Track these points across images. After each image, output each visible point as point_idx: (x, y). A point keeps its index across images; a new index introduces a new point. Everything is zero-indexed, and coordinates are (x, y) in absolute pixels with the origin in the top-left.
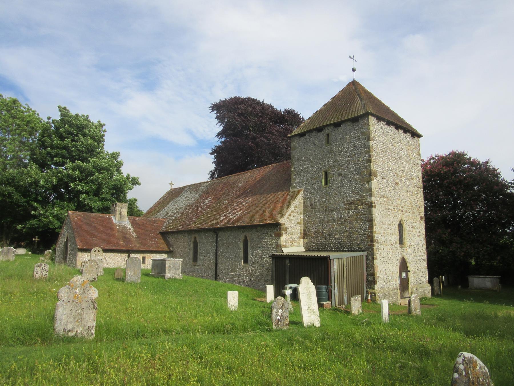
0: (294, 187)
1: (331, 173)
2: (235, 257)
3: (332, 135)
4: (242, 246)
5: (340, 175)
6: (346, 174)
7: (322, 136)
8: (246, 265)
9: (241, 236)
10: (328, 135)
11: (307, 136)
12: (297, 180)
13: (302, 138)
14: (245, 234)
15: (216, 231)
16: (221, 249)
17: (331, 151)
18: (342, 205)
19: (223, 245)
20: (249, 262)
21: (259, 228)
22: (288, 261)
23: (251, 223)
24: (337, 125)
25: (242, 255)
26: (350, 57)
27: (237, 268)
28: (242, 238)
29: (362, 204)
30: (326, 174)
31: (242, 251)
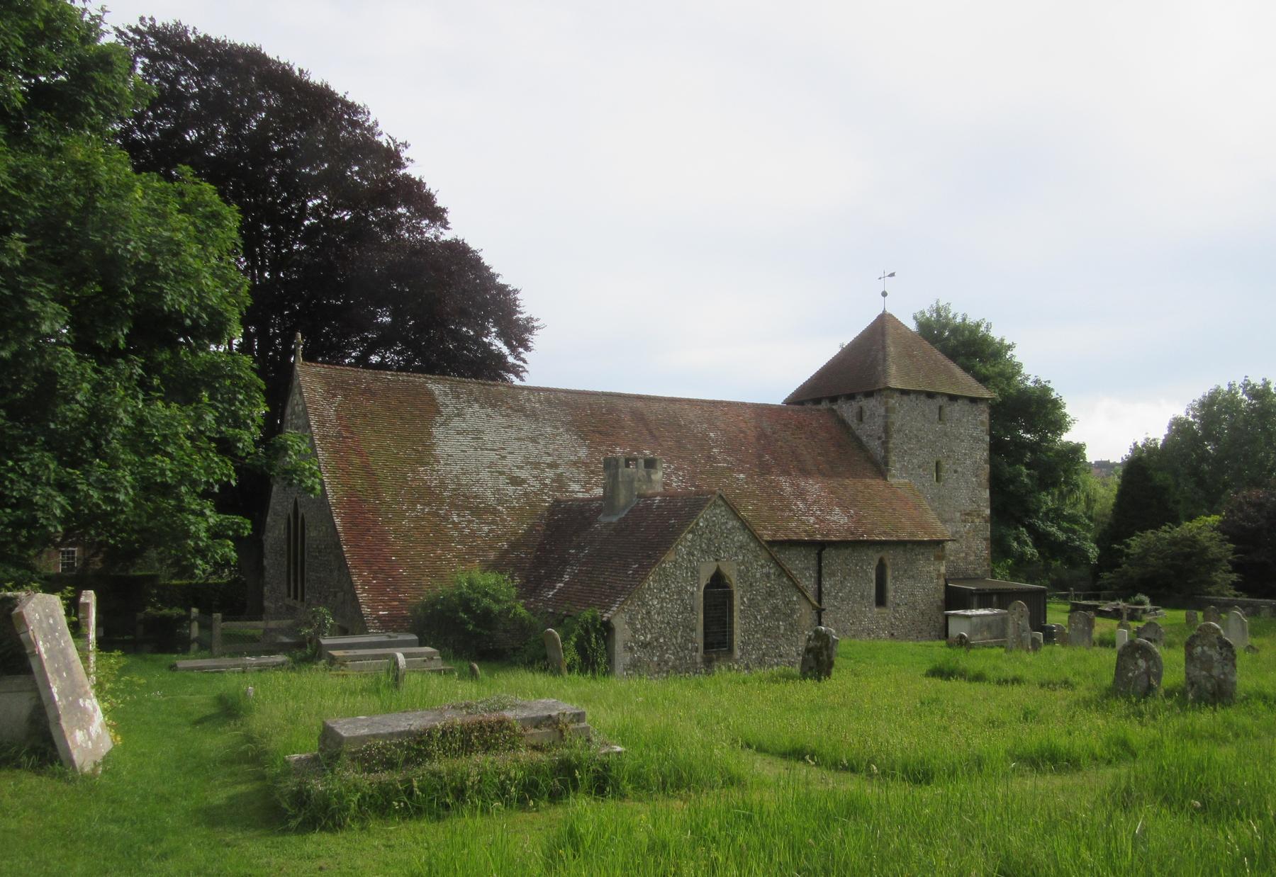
0: (894, 476)
1: (946, 466)
2: (862, 597)
3: (947, 410)
4: (874, 577)
5: (956, 471)
6: (964, 474)
7: (934, 404)
8: (883, 610)
9: (874, 557)
10: (940, 408)
11: (912, 397)
12: (898, 466)
13: (905, 398)
14: (881, 554)
15: (819, 547)
16: (827, 584)
17: (946, 434)
18: (958, 514)
19: (833, 574)
20: (889, 604)
21: (909, 546)
22: (995, 598)
23: (904, 536)
24: (953, 398)
25: (873, 592)
26: (892, 275)
27: (865, 616)
28: (875, 563)
29: (979, 515)
30: (938, 464)
31: (874, 585)
